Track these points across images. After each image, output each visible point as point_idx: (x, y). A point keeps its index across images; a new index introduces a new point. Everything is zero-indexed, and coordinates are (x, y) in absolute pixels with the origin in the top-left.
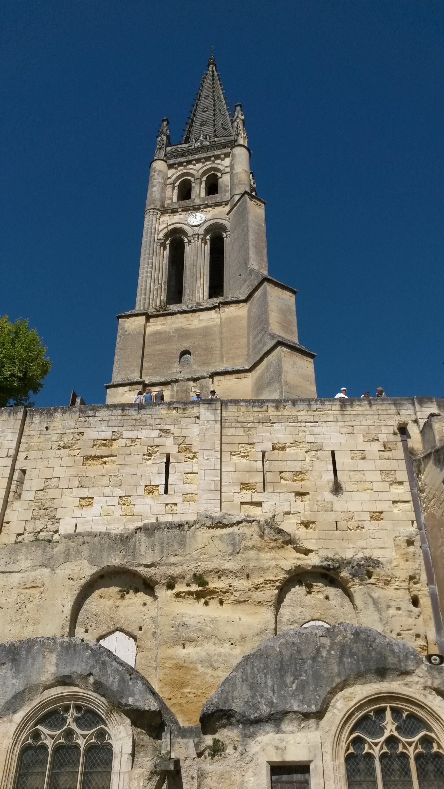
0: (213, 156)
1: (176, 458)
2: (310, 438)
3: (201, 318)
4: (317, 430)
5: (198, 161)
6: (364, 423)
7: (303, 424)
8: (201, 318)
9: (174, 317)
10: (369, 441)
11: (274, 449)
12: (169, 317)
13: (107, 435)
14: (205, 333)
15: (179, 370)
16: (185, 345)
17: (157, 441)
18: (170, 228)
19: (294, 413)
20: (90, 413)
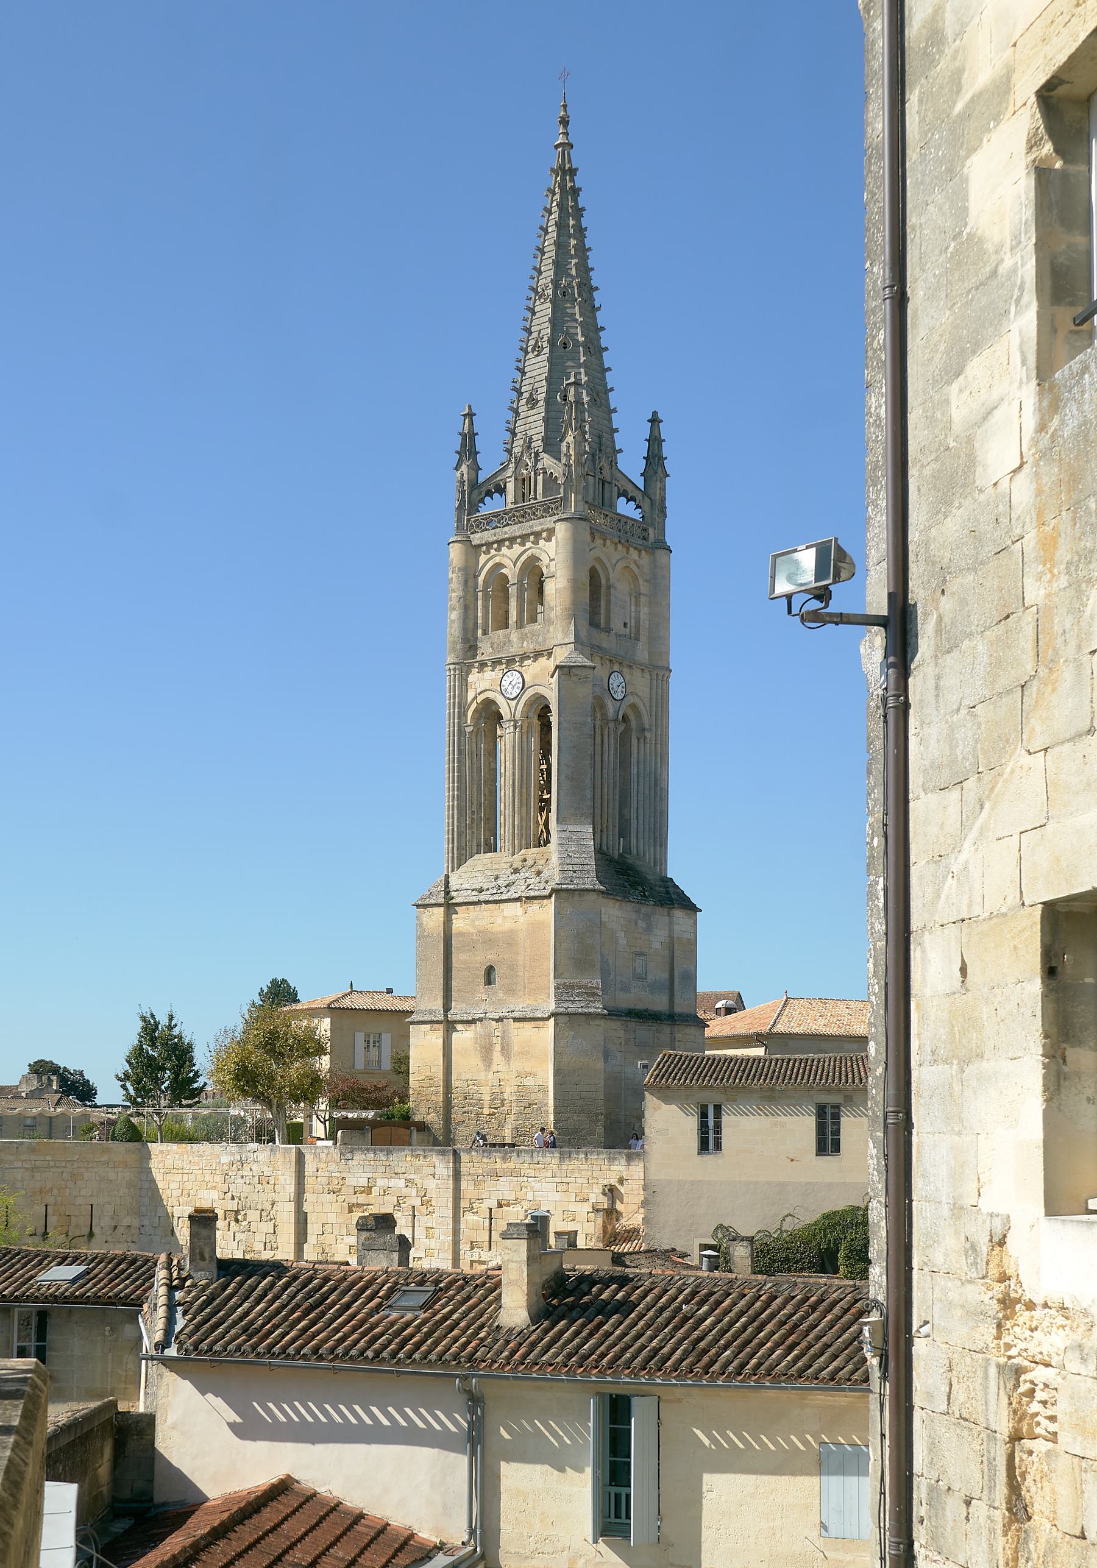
0: (532, 534)
1: (420, 1212)
2: (530, 1196)
3: (506, 913)
4: (537, 1186)
5: (512, 540)
6: (578, 1180)
7: (525, 1179)
8: (506, 913)
9: (477, 907)
10: (580, 1201)
11: (500, 1206)
12: (471, 907)
13: (363, 1182)
14: (510, 939)
15: (484, 997)
16: (491, 957)
17: (405, 1191)
18: (480, 699)
19: (518, 1166)
20: (349, 1156)
